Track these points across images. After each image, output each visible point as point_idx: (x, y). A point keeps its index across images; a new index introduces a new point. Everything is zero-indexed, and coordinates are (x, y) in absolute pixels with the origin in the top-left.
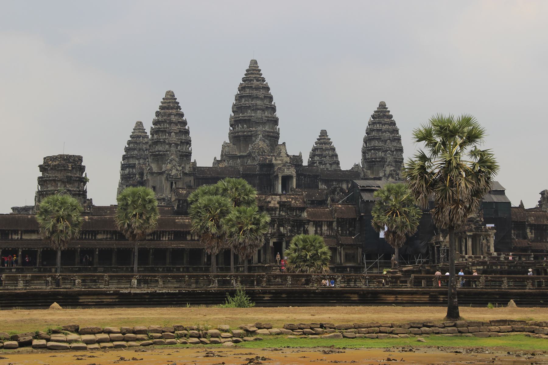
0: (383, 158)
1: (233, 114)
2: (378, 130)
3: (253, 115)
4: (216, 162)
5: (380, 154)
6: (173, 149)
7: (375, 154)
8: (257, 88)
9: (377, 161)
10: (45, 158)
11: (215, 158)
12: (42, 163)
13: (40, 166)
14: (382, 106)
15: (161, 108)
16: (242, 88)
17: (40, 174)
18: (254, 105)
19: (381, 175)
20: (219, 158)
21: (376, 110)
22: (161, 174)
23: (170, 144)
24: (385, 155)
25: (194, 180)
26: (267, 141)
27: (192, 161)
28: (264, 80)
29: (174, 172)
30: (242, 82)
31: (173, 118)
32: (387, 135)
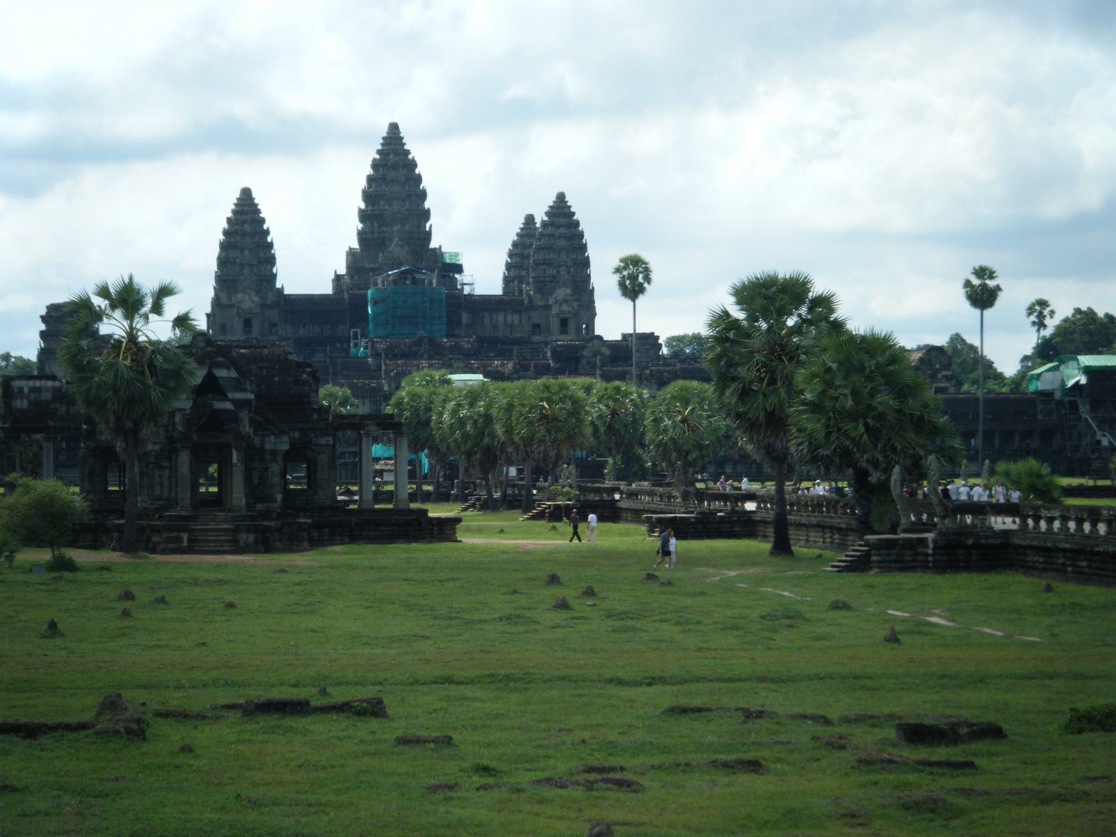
0: (554, 277)
1: (363, 206)
2: (551, 236)
3: (387, 207)
4: (338, 278)
5: (552, 271)
6: (246, 271)
7: (545, 270)
8: (395, 167)
9: (548, 282)
10: (47, 307)
11: (336, 272)
12: (43, 312)
13: (42, 317)
14: (561, 197)
15: (234, 212)
16: (375, 165)
17: (43, 327)
18: (394, 188)
19: (551, 301)
20: (342, 271)
21: (551, 204)
22: (231, 306)
23: (242, 265)
24: (558, 272)
25: (280, 313)
26: (407, 248)
27: (278, 285)
28: (408, 152)
29: (247, 305)
30: (377, 157)
31: (247, 228)
32: (563, 243)
